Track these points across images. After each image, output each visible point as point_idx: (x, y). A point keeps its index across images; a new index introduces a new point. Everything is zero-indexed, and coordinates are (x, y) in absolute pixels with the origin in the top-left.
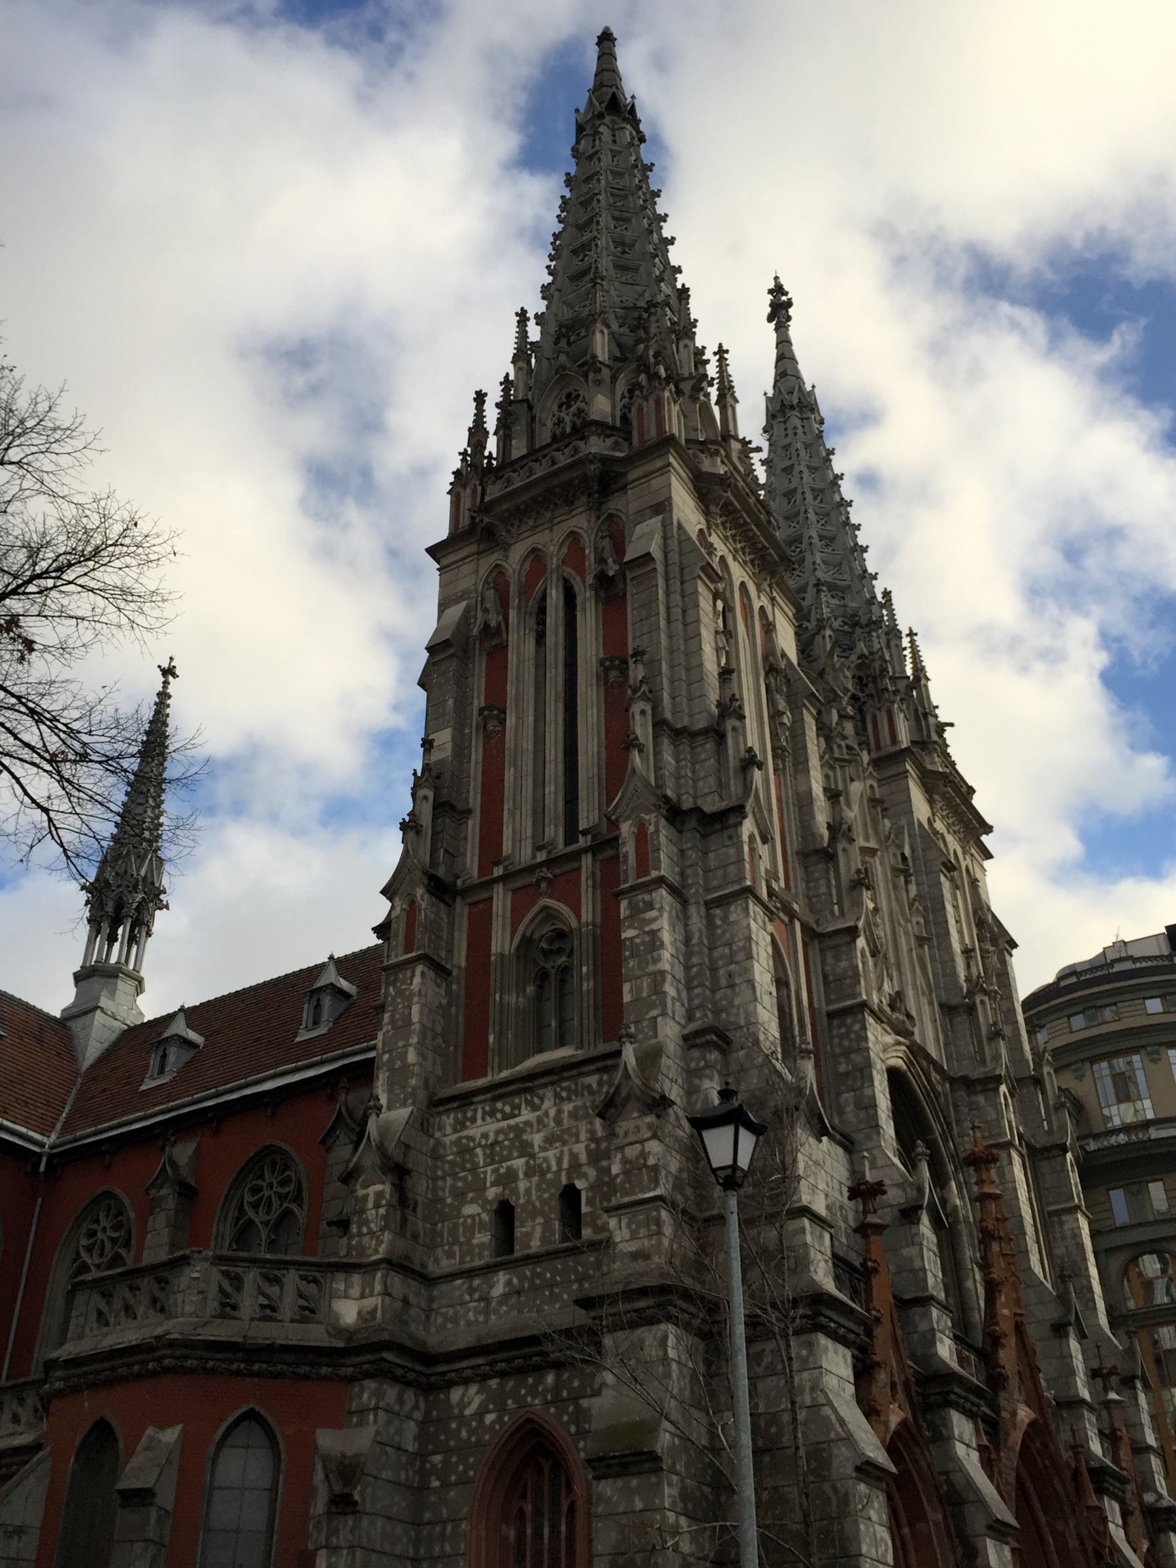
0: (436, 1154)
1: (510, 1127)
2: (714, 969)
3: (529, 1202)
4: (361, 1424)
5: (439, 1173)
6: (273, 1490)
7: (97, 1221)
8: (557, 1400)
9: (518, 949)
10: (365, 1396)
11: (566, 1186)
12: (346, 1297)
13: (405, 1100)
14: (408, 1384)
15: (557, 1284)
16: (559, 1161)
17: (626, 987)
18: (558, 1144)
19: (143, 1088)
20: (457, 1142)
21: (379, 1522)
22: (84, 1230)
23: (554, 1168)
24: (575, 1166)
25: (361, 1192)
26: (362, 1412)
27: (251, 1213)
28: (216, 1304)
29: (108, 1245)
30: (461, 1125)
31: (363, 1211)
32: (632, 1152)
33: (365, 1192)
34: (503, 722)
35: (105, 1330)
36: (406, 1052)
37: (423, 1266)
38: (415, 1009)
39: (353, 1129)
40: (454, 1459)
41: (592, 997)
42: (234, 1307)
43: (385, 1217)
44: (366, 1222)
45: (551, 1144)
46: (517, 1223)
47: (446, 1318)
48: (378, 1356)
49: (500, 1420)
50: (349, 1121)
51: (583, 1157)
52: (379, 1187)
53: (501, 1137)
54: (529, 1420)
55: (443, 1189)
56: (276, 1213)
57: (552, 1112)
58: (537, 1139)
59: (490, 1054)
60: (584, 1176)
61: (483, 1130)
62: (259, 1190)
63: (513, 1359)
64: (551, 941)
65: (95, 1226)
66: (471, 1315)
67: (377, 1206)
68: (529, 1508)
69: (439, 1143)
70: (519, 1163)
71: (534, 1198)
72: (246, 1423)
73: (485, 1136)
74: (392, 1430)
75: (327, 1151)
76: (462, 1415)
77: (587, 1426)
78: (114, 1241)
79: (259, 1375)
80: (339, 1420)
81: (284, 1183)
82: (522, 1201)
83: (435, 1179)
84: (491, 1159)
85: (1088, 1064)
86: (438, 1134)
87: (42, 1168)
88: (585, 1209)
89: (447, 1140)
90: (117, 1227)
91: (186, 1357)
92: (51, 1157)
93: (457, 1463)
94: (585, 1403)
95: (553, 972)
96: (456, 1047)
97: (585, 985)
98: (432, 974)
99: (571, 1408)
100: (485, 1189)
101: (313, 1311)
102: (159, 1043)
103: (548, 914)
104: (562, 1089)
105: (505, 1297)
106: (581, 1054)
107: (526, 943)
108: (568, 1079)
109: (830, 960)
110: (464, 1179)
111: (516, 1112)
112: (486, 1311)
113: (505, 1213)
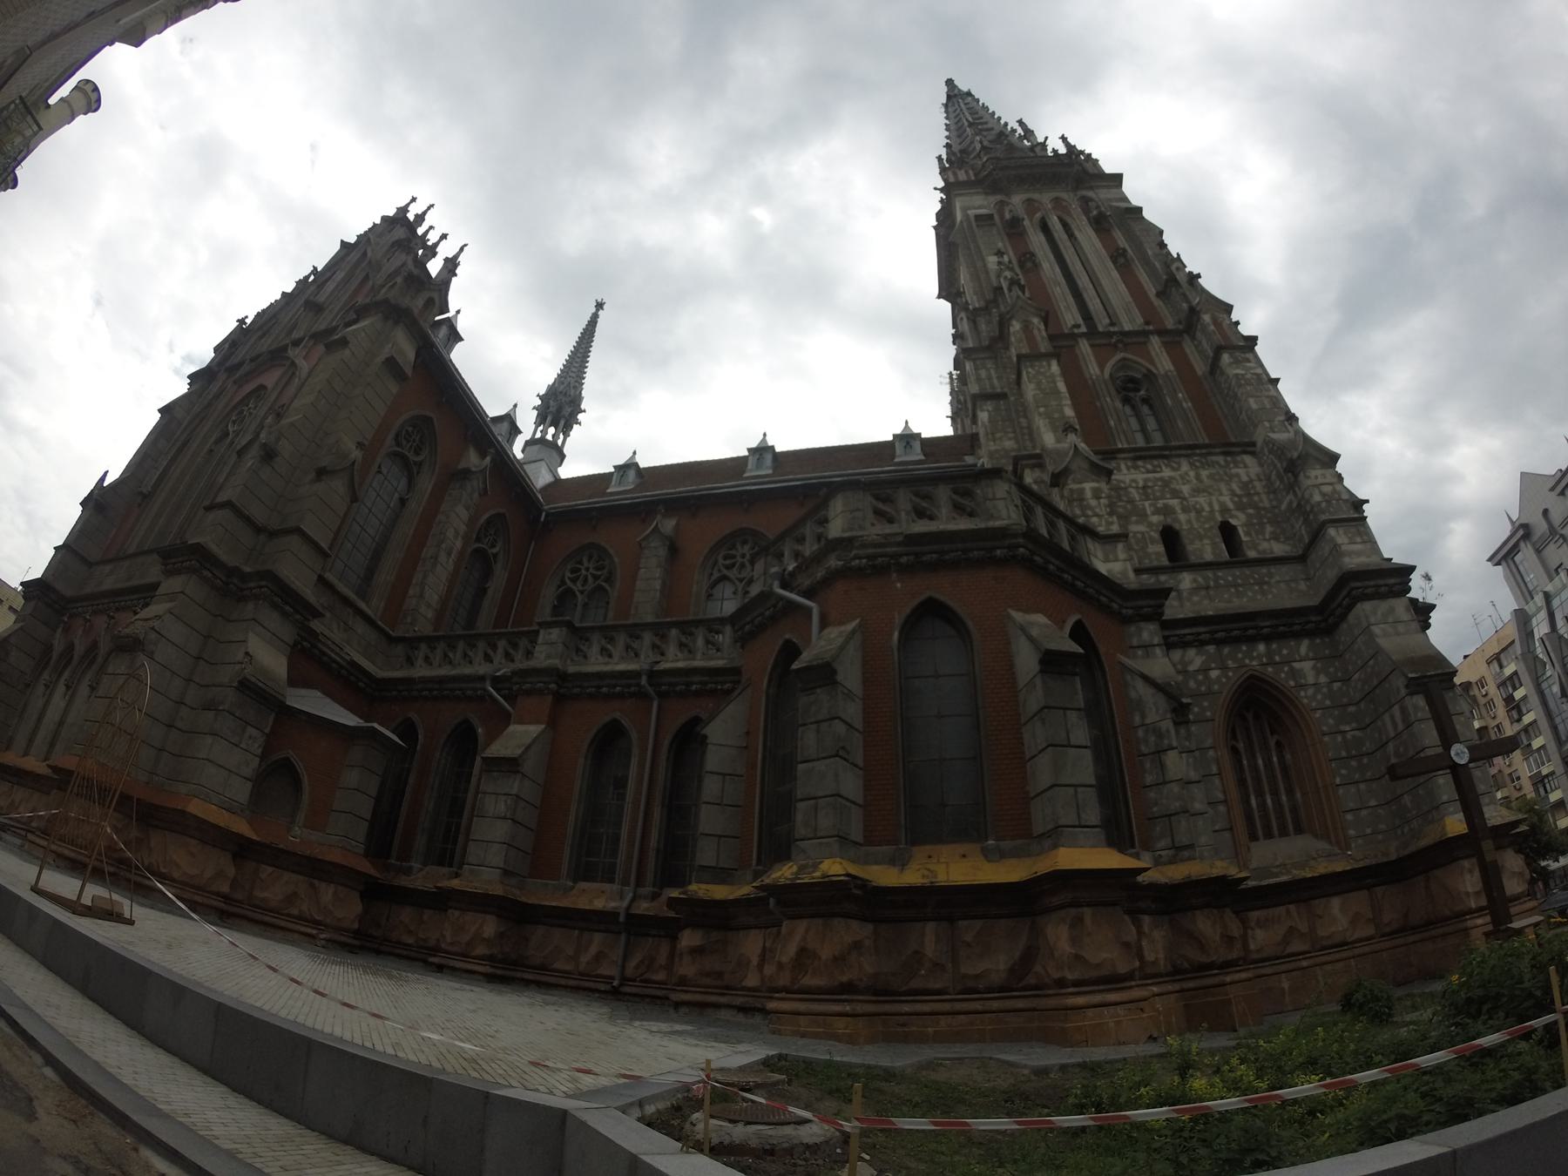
4: (1147, 656)
7: (580, 563)
10: (1145, 635)
11: (1221, 522)
15: (1239, 585)
16: (1210, 504)
18: (1205, 494)
22: (569, 567)
23: (1207, 508)
24: (1224, 510)
29: (590, 579)
32: (1327, 489)
44: (1091, 508)
51: (1231, 506)
53: (1150, 484)
60: (1237, 517)
62: (734, 557)
63: (1232, 630)
70: (1174, 502)
73: (1134, 481)
77: (1303, 681)
78: (596, 578)
87: (542, 519)
88: (1244, 538)
90: (597, 569)
94: (1296, 665)
99: (1286, 669)
105: (1195, 591)
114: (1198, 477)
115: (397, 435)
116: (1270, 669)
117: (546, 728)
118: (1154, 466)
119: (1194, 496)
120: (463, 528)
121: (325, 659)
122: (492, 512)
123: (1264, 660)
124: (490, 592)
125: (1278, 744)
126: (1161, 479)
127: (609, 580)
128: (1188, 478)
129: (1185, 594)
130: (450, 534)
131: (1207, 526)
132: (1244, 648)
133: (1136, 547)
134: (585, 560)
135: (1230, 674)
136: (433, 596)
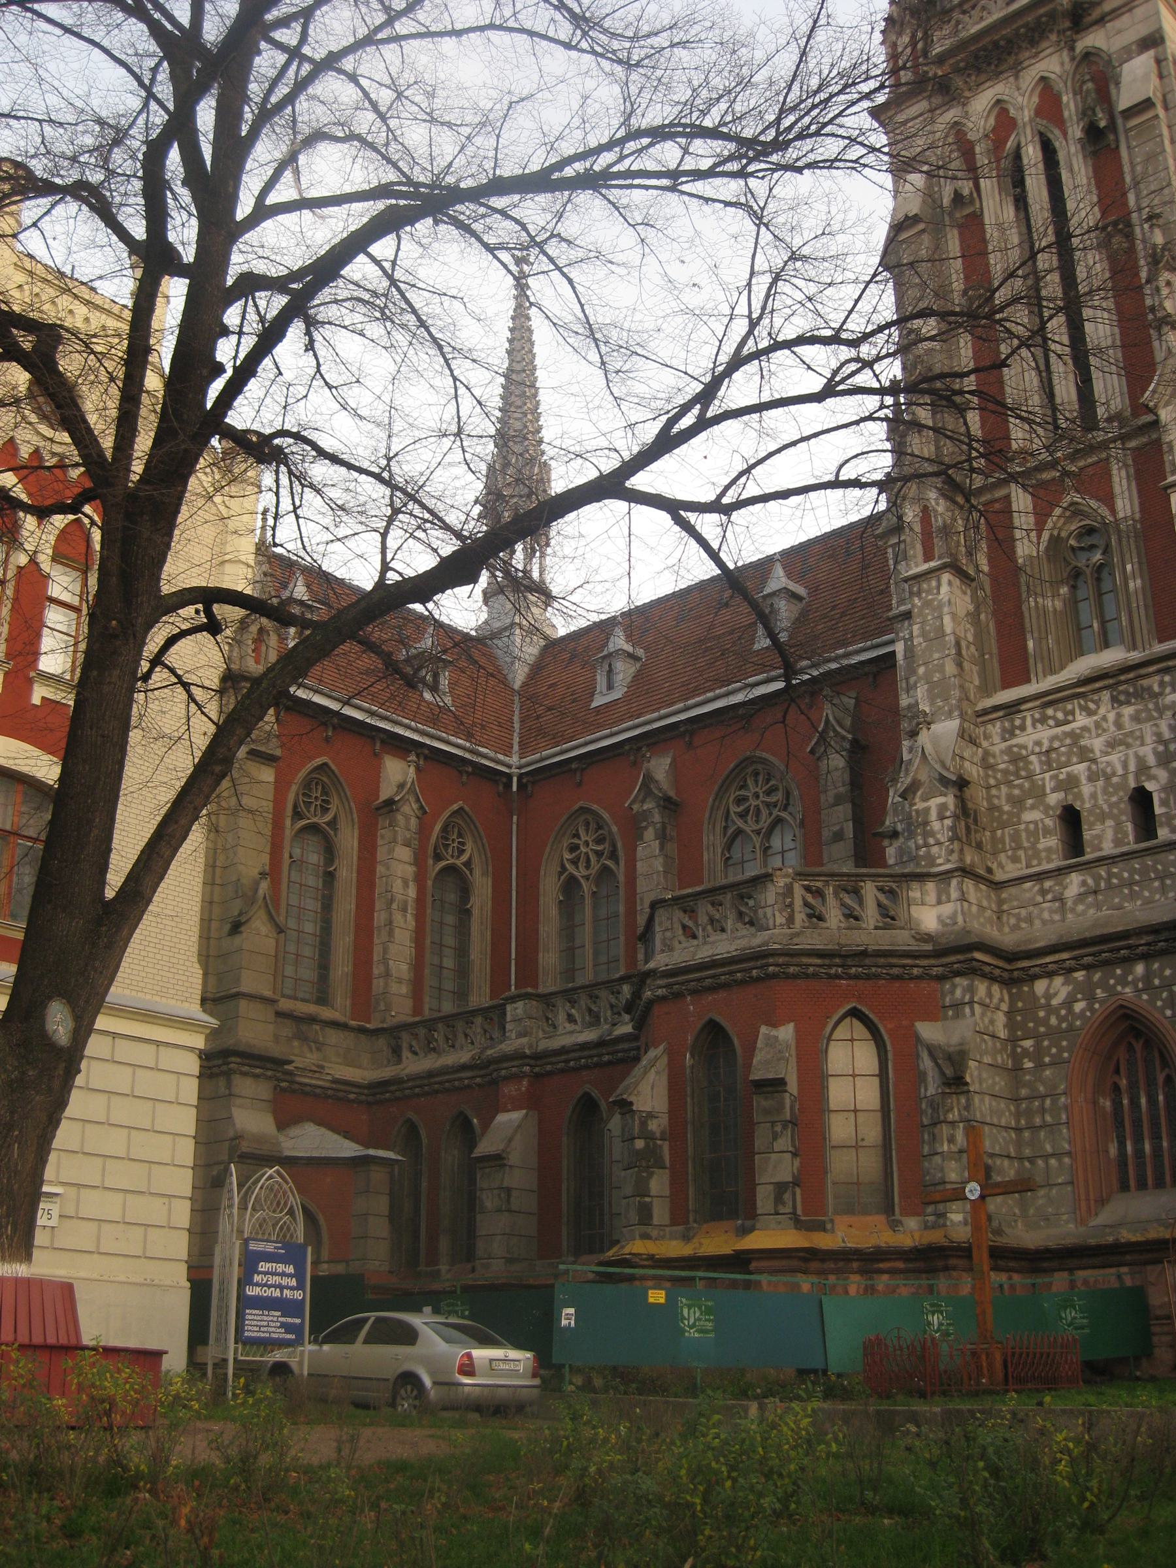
0: (986, 764)
1: (1066, 734)
3: (1095, 806)
4: (958, 1015)
5: (992, 782)
6: (883, 1075)
7: (577, 836)
8: (1149, 987)
9: (1047, 549)
10: (958, 993)
12: (923, 904)
13: (950, 712)
14: (993, 979)
15: (1136, 883)
16: (1125, 765)
19: (594, 705)
21: (987, 1098)
22: (566, 843)
24: (1143, 769)
26: (957, 1006)
27: (740, 823)
28: (803, 916)
29: (593, 858)
31: (926, 823)
33: (925, 805)
35: (695, 942)
36: (943, 665)
37: (990, 871)
38: (947, 620)
39: (844, 738)
40: (1046, 1043)
41: (1141, 597)
42: (820, 918)
43: (953, 828)
44: (932, 834)
45: (1113, 747)
46: (1085, 827)
47: (1018, 918)
48: (969, 956)
49: (1090, 1007)
50: (839, 729)
51: (1151, 760)
52: (940, 800)
53: (1056, 744)
54: (1122, 1006)
55: (998, 797)
56: (765, 821)
57: (1111, 716)
59: (1031, 661)
60: (1154, 778)
61: (1035, 737)
62: (745, 799)
64: (1080, 537)
65: (576, 841)
66: (1046, 915)
67: (941, 818)
68: (1124, 1082)
69: (987, 753)
70: (1080, 769)
71: (1101, 802)
72: (848, 1020)
73: (1038, 743)
74: (986, 1020)
75: (819, 759)
76: (1048, 1006)
78: (599, 854)
79: (856, 977)
80: (934, 1013)
81: (768, 793)
82: (1087, 805)
83: (988, 788)
84: (1048, 765)
86: (985, 744)
87: (515, 788)
88: (1158, 810)
89: (996, 749)
90: (599, 841)
91: (788, 965)
92: (520, 777)
93: (1049, 1048)
95: (1088, 571)
96: (991, 654)
97: (1131, 585)
98: (957, 582)
99: (1165, 995)
100: (1045, 795)
101: (893, 919)
102: (604, 657)
103: (1075, 511)
104: (1120, 692)
105: (1081, 898)
106: (1135, 656)
107: (1055, 541)
108: (1126, 682)
110: (1021, 787)
111: (1070, 718)
112: (1063, 909)
113: (1071, 819)
114: (1119, 725)
115: (295, 806)
116: (1145, 997)
117: (526, 1115)
118: (1066, 714)
119: (1107, 754)
120: (410, 870)
121: (308, 1089)
122: (446, 814)
123: (1140, 985)
124: (476, 912)
125: (1168, 1079)
126: (1071, 734)
127: (613, 855)
128: (1105, 725)
129: (1069, 904)
130: (398, 886)
131: (1114, 799)
132: (1119, 971)
133: (1026, 844)
134: (582, 832)
135: (1097, 1006)
136: (401, 967)
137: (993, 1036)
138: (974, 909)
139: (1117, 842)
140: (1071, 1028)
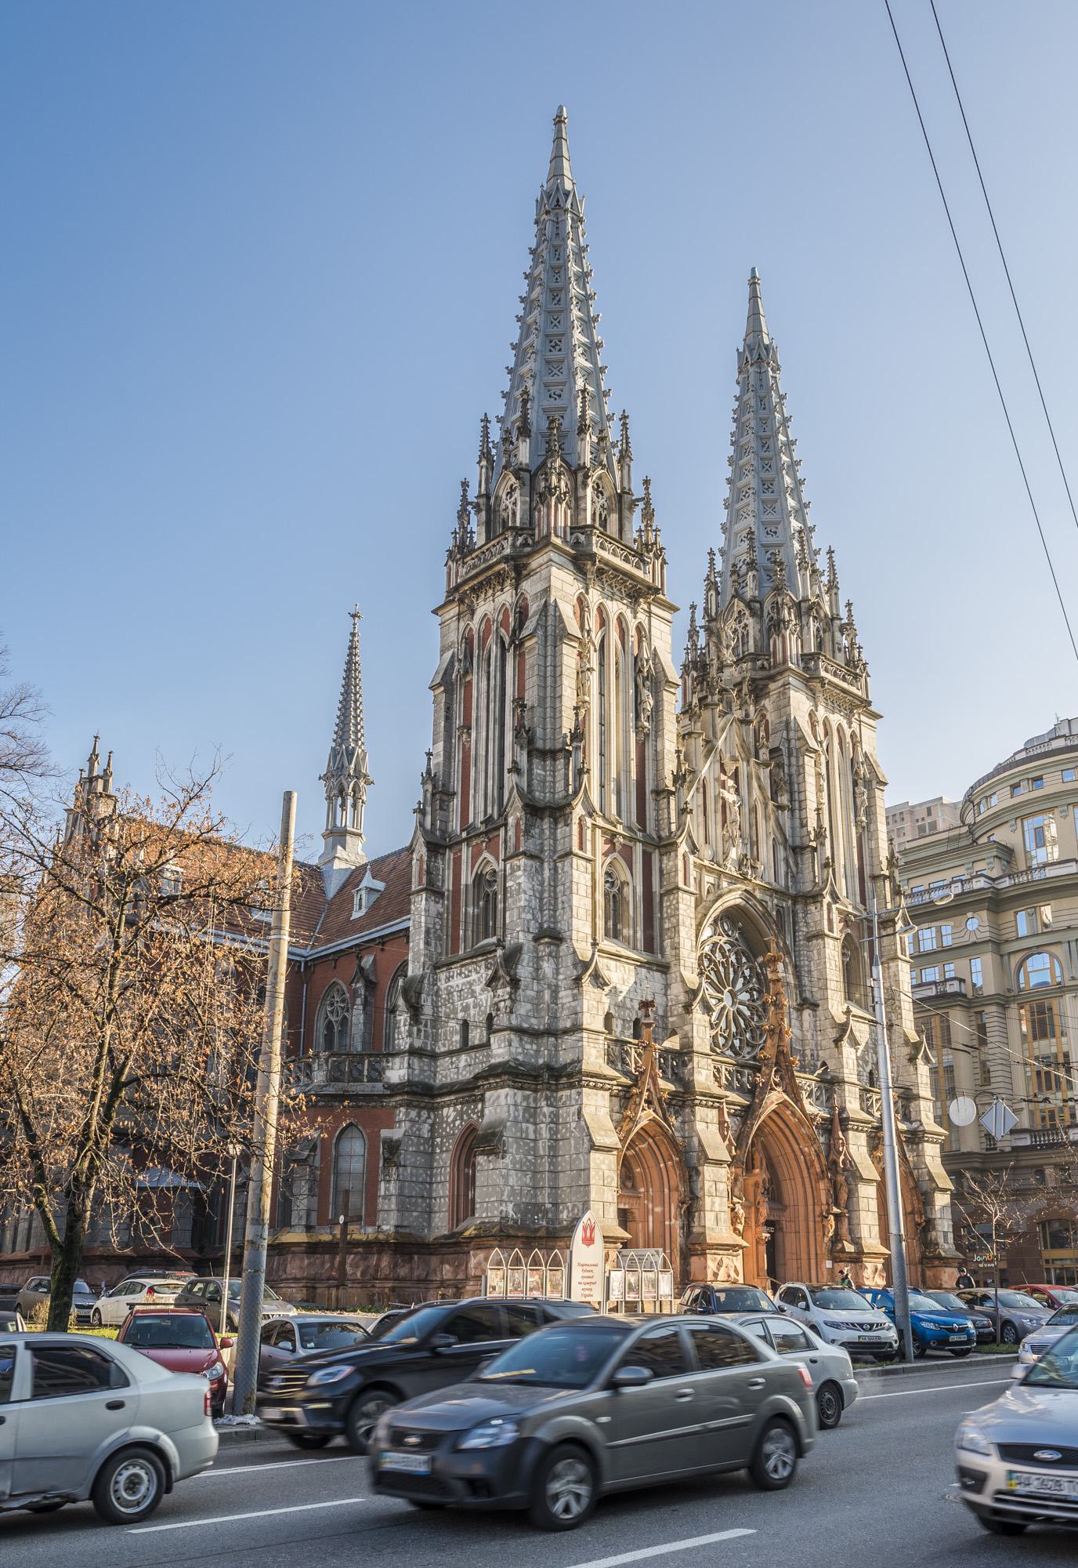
2: (556, 899)
17: (508, 914)
20: (446, 989)
25: (398, 1018)
26: (400, 1122)
30: (448, 979)
34: (469, 735)
58: (478, 988)
69: (439, 989)
70: (471, 1001)
85: (1019, 821)
89: (442, 987)
107: (479, 878)
109: (665, 861)
112: (458, 1073)
113: (465, 1025)
126: (469, 983)
137: (419, 1137)
138: (417, 1072)
139: (480, 1040)
140: (454, 1134)
